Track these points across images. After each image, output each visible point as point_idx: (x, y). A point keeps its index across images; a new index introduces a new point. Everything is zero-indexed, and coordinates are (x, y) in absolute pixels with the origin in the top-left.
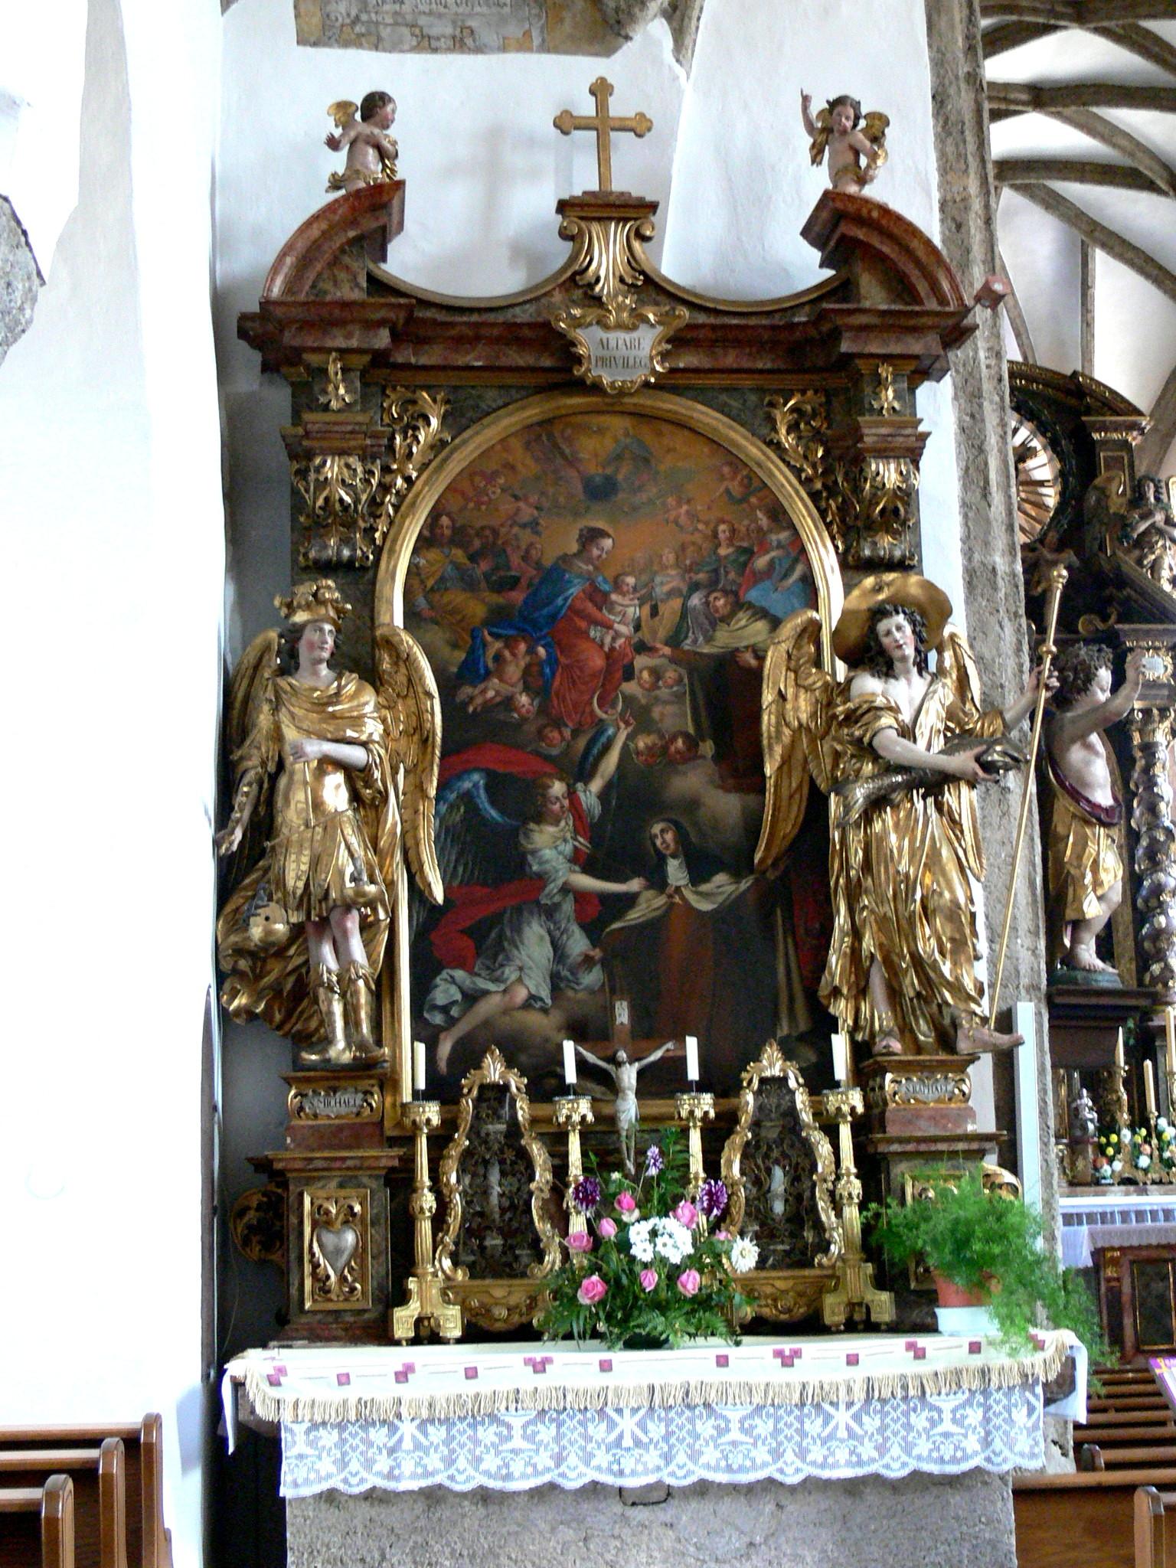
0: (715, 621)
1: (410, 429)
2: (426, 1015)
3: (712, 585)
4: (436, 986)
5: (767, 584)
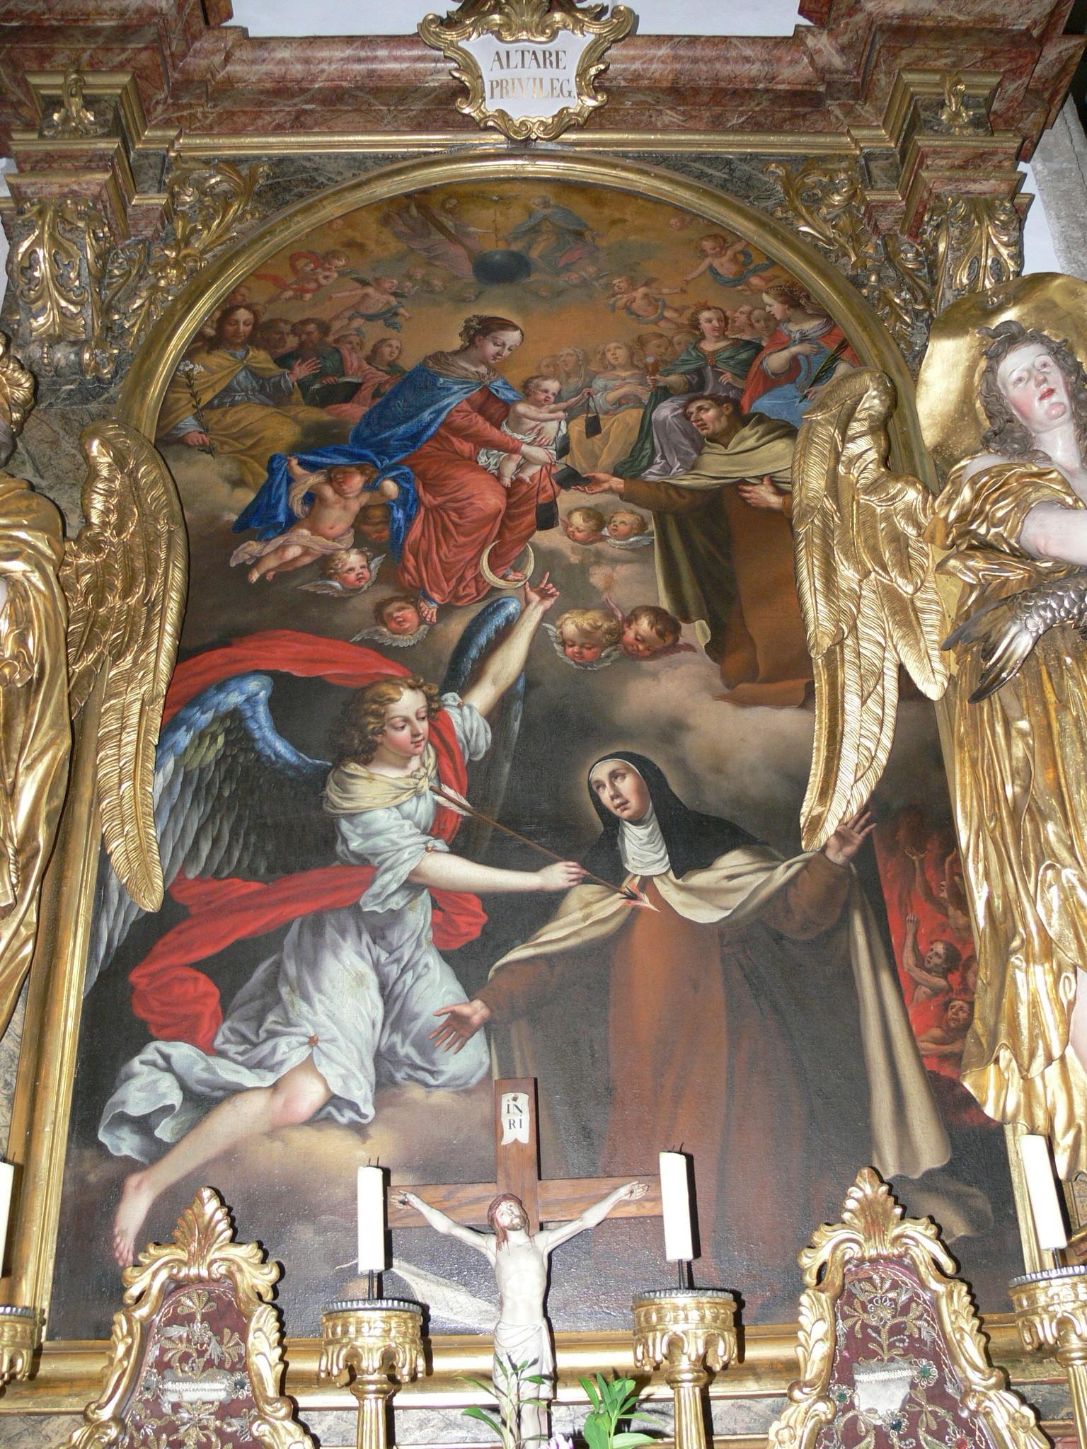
2: (103, 1137)
3: (695, 388)
4: (130, 1077)
5: (788, 390)
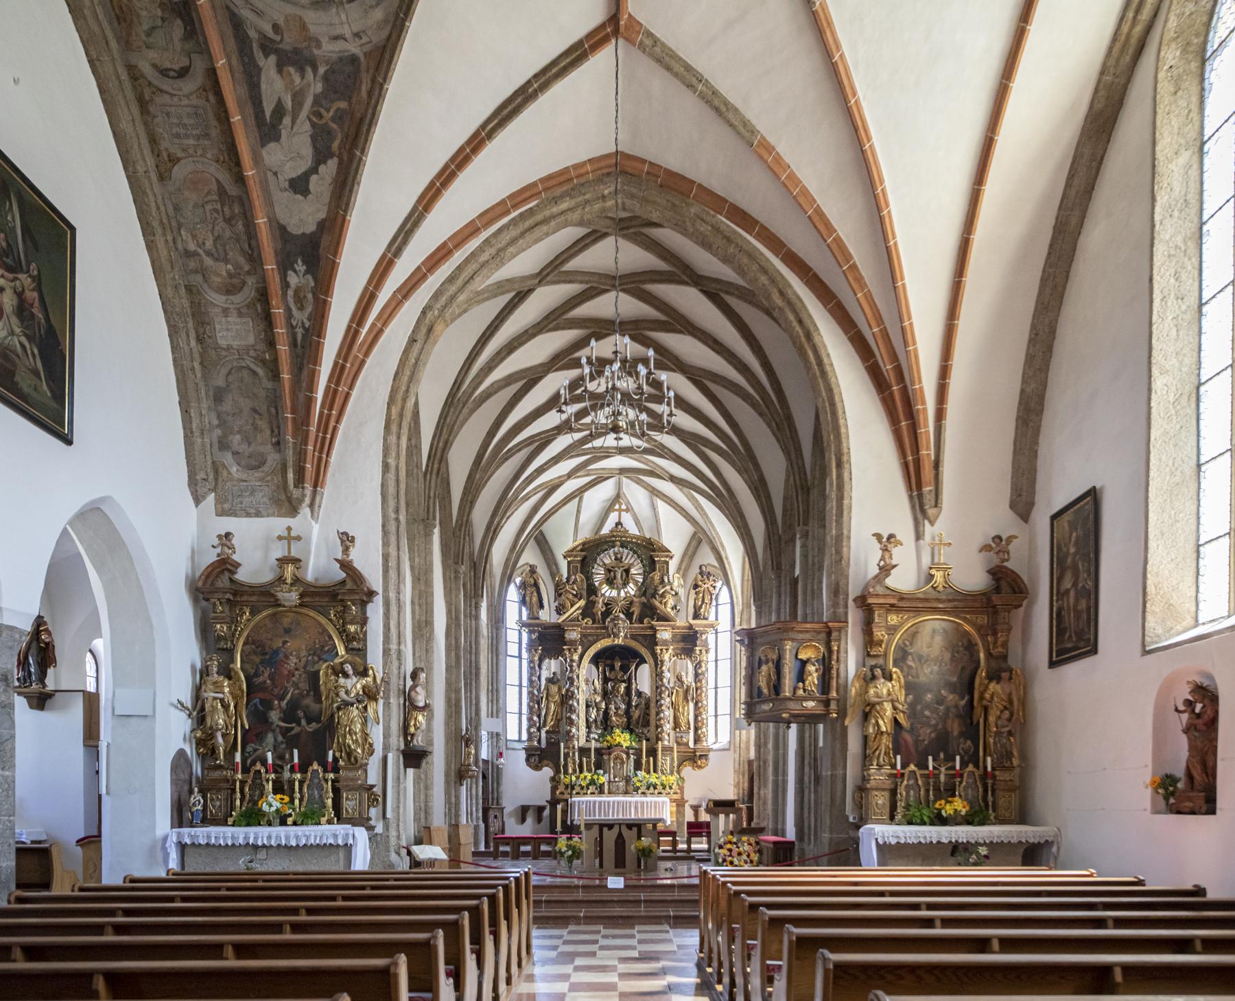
0: (315, 663)
1: (241, 618)
3: (314, 654)
